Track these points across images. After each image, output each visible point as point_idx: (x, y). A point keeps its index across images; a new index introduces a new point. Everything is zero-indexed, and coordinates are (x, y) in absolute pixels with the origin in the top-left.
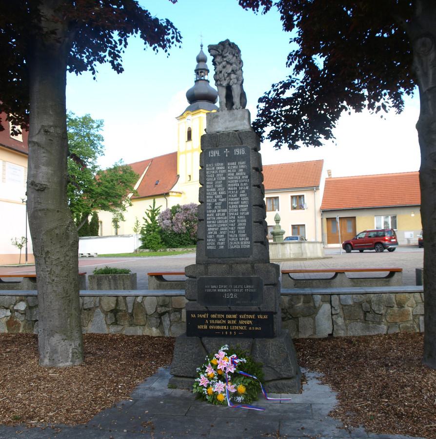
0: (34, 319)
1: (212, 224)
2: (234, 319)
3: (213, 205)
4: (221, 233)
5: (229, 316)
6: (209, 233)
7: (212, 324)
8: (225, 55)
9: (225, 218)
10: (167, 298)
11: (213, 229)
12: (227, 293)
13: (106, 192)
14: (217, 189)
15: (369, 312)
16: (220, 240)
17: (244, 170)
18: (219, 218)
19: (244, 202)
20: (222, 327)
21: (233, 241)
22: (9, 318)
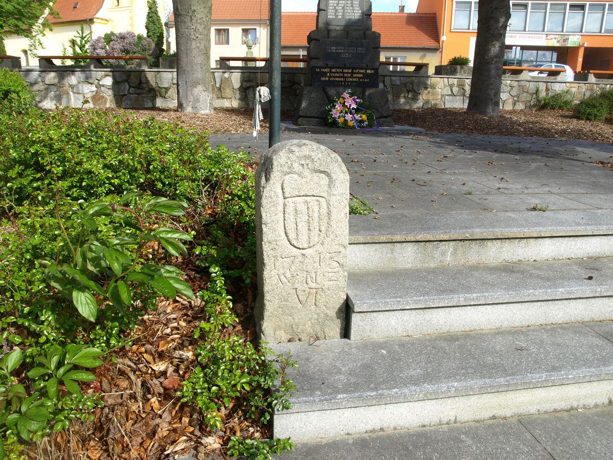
0: (122, 94)
2: (349, 73)
4: (340, 5)
5: (346, 71)
6: (330, 5)
7: (332, 77)
12: (343, 53)
13: (19, 11)
16: (339, 11)
22: (94, 93)
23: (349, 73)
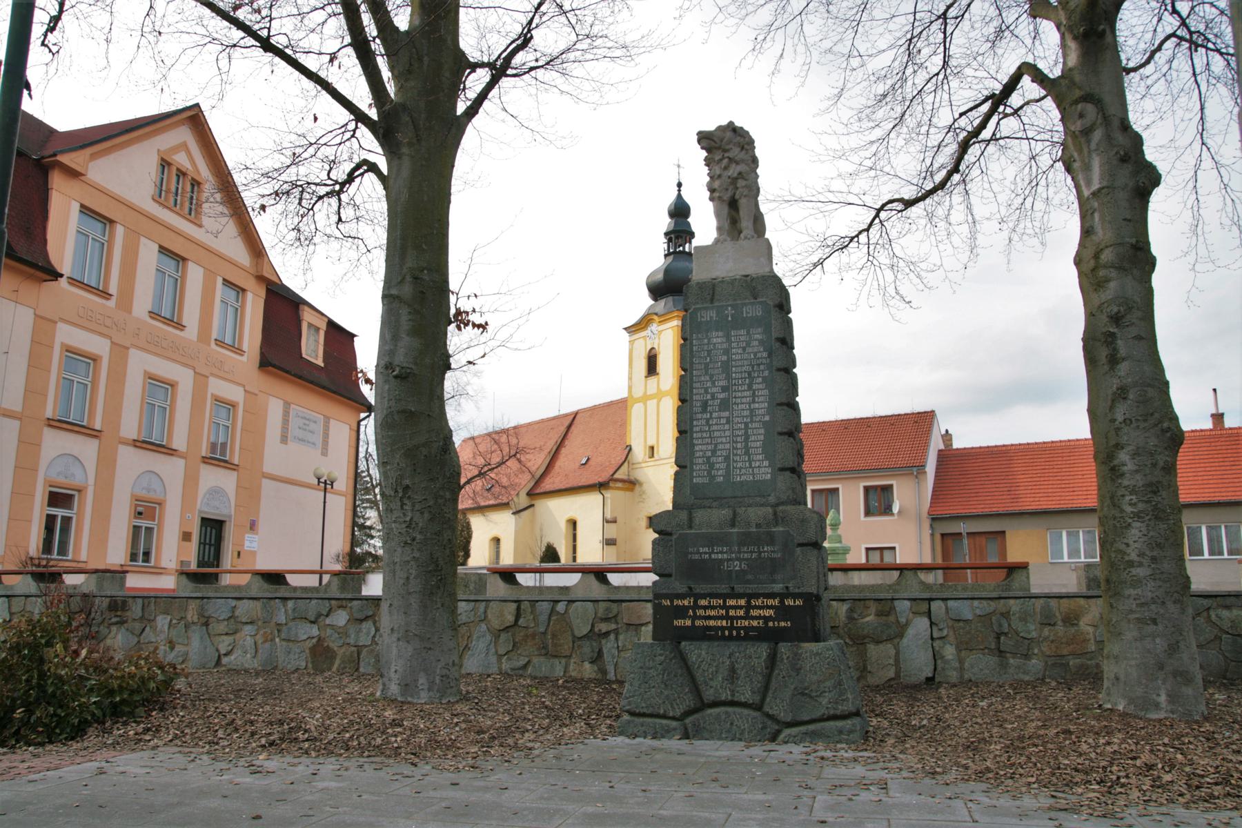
1: (702, 438)
2: (741, 607)
3: (705, 405)
4: (719, 453)
6: (697, 454)
8: (727, 147)
9: (727, 427)
10: (614, 606)
11: (704, 447)
12: (728, 560)
14: (712, 376)
15: (1006, 634)
16: (717, 466)
17: (761, 342)
18: (715, 428)
19: (761, 399)
20: (719, 623)
21: (741, 468)
22: (314, 641)
23: (741, 607)
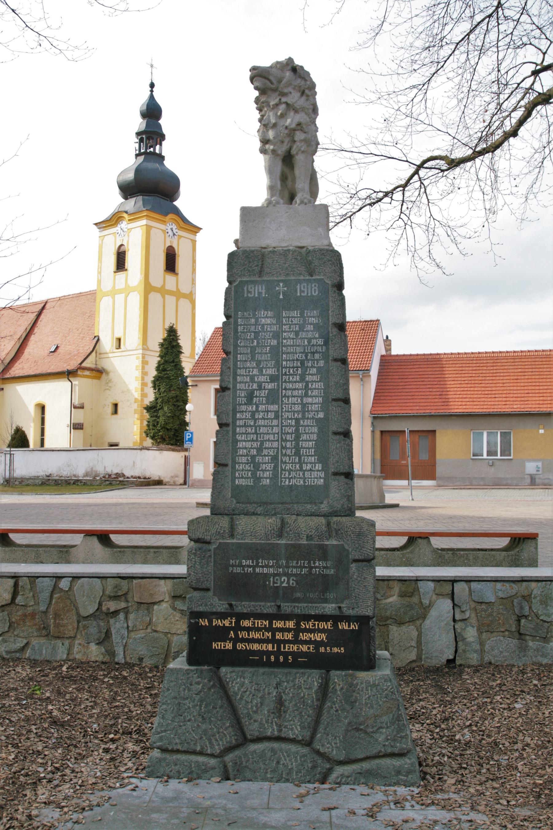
1: (247, 434)
2: (289, 630)
3: (250, 396)
4: (265, 452)
5: (279, 624)
6: (241, 452)
7: (243, 640)
8: (286, 91)
9: (275, 422)
10: (124, 583)
11: (248, 445)
12: (275, 575)
14: (259, 363)
15: (526, 617)
17: (317, 327)
18: (261, 422)
19: (315, 393)
20: (264, 647)
21: (290, 471)
23: (289, 630)
